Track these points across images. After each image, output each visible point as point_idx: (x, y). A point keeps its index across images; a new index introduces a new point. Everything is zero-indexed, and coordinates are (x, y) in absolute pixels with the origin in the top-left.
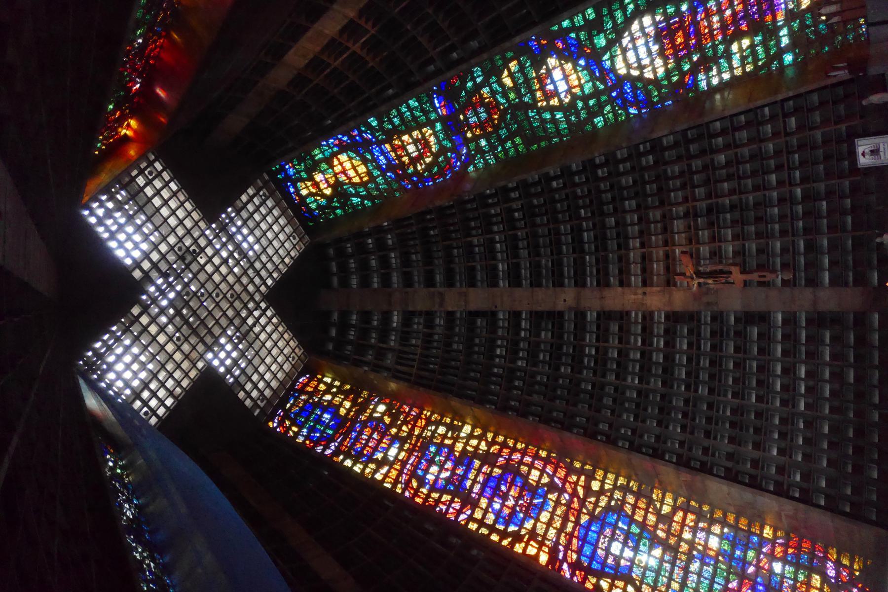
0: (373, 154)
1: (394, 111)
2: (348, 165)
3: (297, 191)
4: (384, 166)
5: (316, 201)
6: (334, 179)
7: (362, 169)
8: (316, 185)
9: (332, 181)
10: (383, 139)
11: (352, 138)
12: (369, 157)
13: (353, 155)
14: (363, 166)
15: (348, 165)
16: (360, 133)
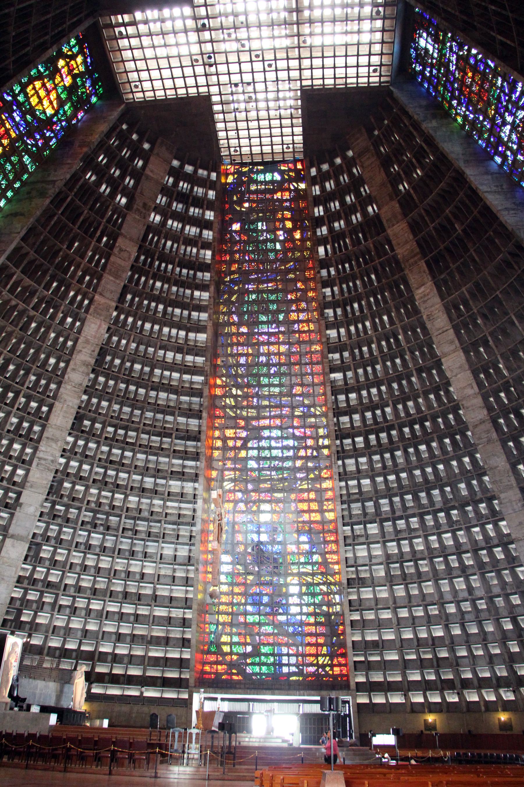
0: (26, 121)
1: (11, 178)
2: (46, 103)
3: (85, 62)
4: (15, 108)
5: (70, 50)
6: (56, 82)
7: (34, 101)
8: (70, 71)
9: (58, 79)
10: (18, 142)
11: (43, 136)
12: (28, 117)
13: (42, 117)
14: (34, 104)
15: (46, 103)
16: (36, 145)
